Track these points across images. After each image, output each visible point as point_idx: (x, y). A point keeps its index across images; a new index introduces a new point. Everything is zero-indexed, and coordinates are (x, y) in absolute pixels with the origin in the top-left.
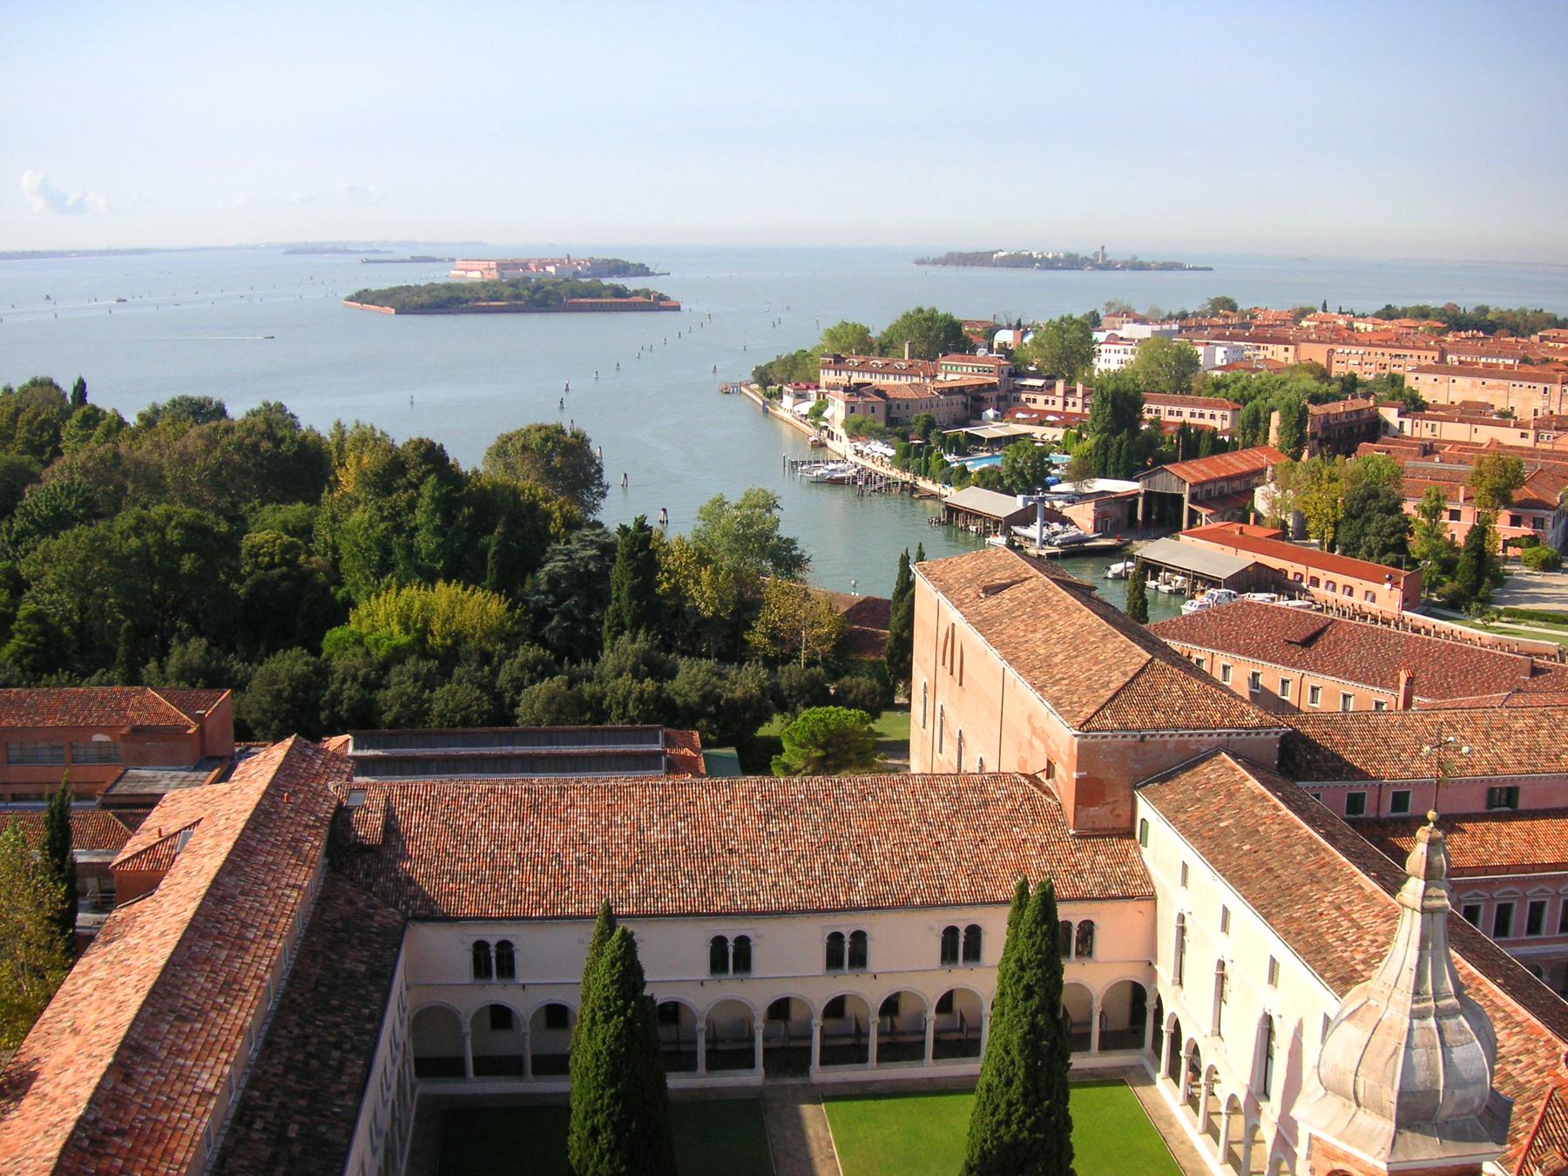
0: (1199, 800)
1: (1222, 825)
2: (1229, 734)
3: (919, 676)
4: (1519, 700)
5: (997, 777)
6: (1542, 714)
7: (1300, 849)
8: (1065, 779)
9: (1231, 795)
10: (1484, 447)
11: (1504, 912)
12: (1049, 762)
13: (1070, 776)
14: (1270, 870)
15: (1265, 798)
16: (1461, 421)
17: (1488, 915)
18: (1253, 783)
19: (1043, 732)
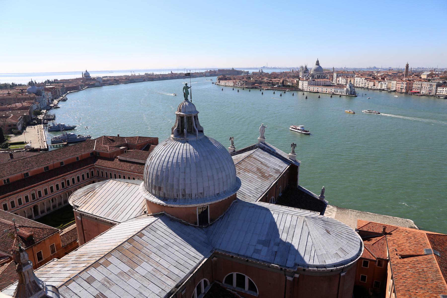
11: (12, 203)
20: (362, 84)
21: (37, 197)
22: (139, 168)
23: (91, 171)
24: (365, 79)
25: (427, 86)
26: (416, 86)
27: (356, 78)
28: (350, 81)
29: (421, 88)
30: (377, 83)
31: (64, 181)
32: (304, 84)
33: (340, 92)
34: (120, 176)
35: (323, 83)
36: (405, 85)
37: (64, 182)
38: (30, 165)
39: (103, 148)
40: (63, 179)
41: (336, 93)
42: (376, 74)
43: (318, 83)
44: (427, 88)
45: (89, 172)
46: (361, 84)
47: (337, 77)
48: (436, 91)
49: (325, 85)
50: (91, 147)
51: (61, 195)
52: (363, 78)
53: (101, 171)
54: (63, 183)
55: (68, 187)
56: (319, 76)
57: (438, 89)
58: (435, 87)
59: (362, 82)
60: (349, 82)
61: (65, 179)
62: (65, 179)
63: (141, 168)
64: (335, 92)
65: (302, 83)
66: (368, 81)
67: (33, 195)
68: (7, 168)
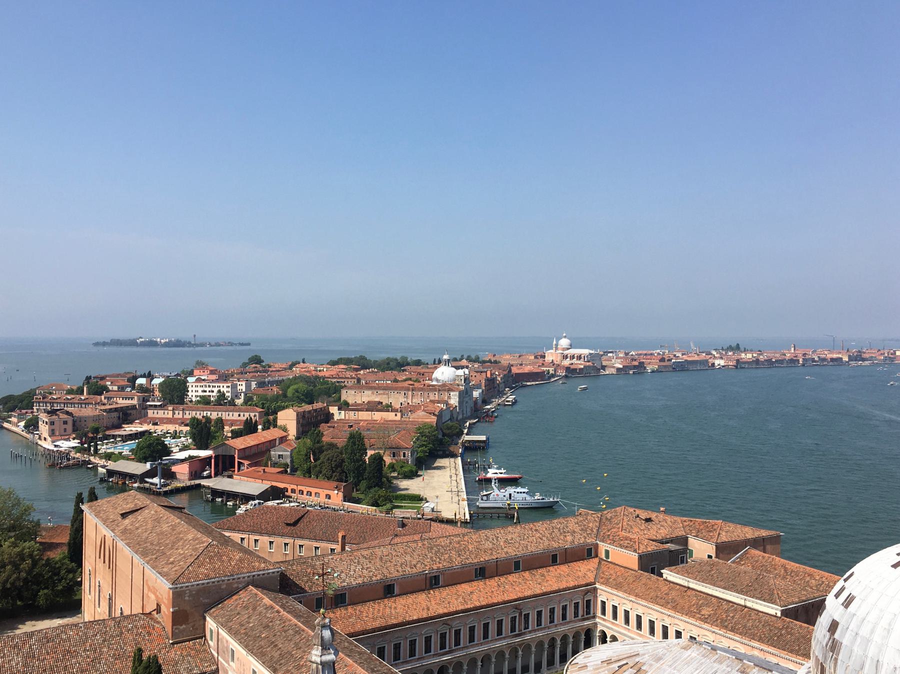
0: (238, 614)
1: (251, 625)
2: (254, 576)
3: (88, 565)
4: (397, 540)
5: (128, 617)
6: (406, 546)
7: (291, 632)
8: (167, 613)
9: (254, 609)
10: (378, 422)
11: (397, 647)
12: (158, 605)
13: (168, 610)
14: (276, 646)
15: (272, 607)
16: (367, 410)
17: (389, 651)
18: (267, 601)
19: (154, 588)
21: (450, 645)
22: (727, 617)
23: (585, 599)
31: (517, 615)
34: (665, 630)
37: (518, 617)
38: (446, 556)
39: (622, 540)
40: (516, 609)
45: (580, 601)
50: (589, 534)
51: (503, 652)
53: (612, 603)
54: (513, 620)
55: (524, 634)
61: (521, 610)
62: (521, 610)
63: (733, 617)
67: (443, 636)
68: (397, 556)
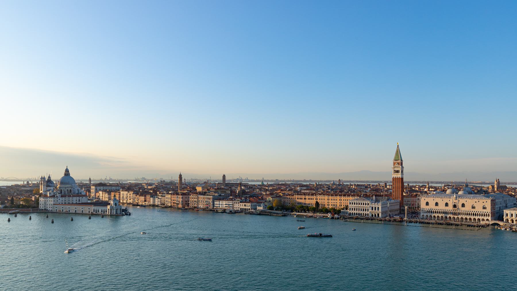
20: (130, 200)
24: (133, 194)
25: (203, 200)
26: (192, 200)
27: (122, 193)
28: (115, 196)
29: (198, 202)
30: (148, 197)
32: (48, 203)
33: (102, 211)
35: (76, 200)
36: (181, 200)
41: (96, 213)
42: (146, 187)
43: (69, 200)
44: (204, 202)
46: (129, 199)
47: (97, 191)
48: (213, 204)
49: (80, 202)
52: (131, 192)
56: (70, 190)
57: (215, 203)
58: (212, 200)
59: (130, 197)
60: (112, 198)
64: (95, 212)
65: (44, 201)
66: (138, 196)
